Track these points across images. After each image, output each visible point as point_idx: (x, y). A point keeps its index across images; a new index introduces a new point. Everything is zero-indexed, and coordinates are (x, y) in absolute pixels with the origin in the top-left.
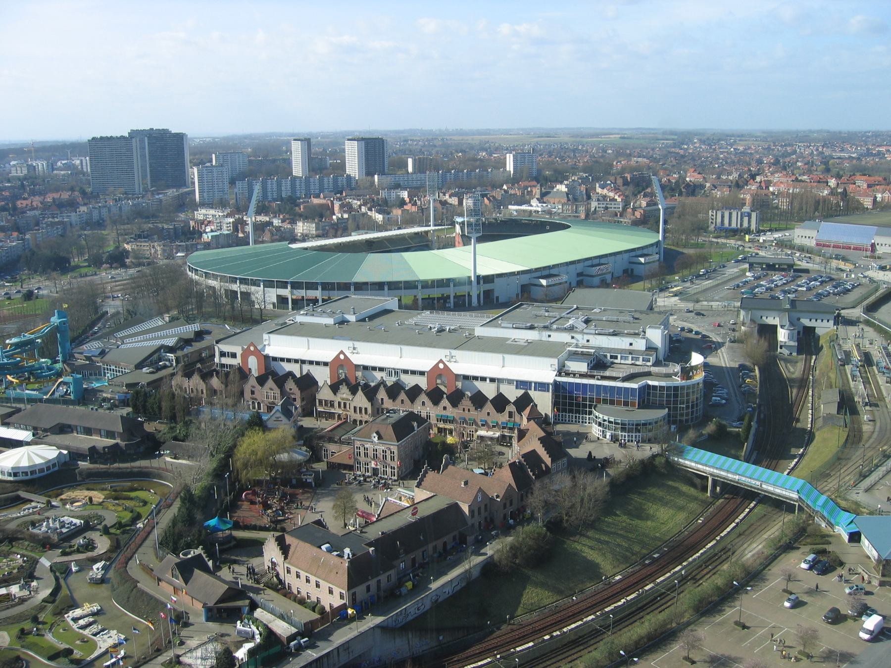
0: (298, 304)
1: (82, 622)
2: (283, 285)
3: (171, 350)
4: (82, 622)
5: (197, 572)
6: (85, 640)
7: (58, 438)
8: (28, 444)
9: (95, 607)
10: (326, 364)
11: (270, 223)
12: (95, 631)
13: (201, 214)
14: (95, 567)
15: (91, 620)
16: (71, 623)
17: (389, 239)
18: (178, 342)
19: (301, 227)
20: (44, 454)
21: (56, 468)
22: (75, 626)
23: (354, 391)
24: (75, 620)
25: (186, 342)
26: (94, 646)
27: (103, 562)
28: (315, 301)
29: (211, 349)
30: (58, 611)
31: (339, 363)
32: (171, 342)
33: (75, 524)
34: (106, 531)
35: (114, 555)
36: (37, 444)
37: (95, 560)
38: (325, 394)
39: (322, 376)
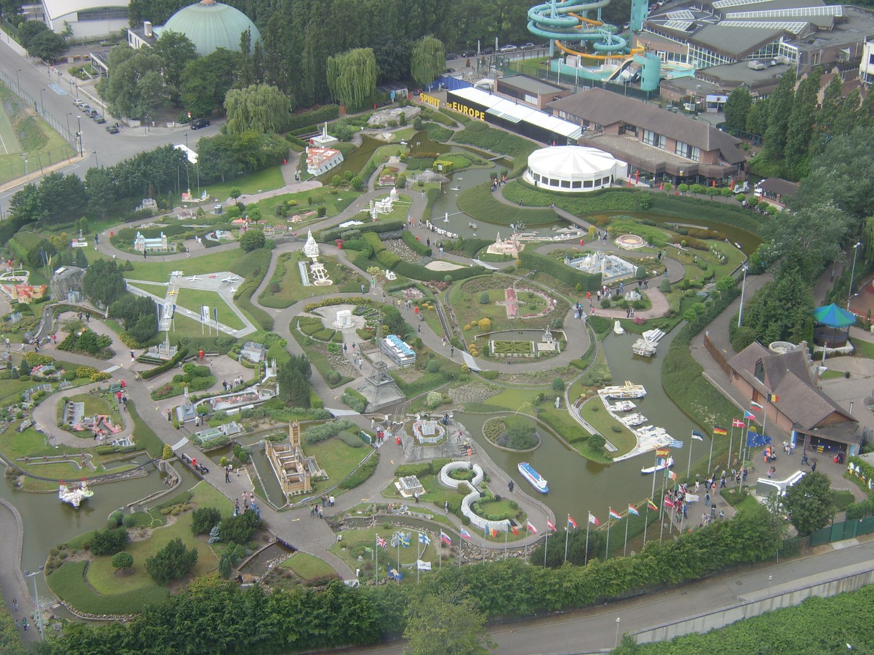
1: (620, 406)
3: (790, 37)
4: (620, 406)
5: (790, 376)
6: (618, 430)
7: (617, 142)
8: (574, 143)
9: (640, 391)
12: (637, 421)
14: (645, 334)
15: (632, 405)
16: (606, 403)
18: (804, 31)
22: (610, 409)
24: (612, 400)
26: (632, 442)
27: (657, 331)
30: (590, 381)
32: (796, 27)
33: (625, 269)
34: (666, 289)
35: (673, 322)
36: (586, 145)
37: (646, 325)
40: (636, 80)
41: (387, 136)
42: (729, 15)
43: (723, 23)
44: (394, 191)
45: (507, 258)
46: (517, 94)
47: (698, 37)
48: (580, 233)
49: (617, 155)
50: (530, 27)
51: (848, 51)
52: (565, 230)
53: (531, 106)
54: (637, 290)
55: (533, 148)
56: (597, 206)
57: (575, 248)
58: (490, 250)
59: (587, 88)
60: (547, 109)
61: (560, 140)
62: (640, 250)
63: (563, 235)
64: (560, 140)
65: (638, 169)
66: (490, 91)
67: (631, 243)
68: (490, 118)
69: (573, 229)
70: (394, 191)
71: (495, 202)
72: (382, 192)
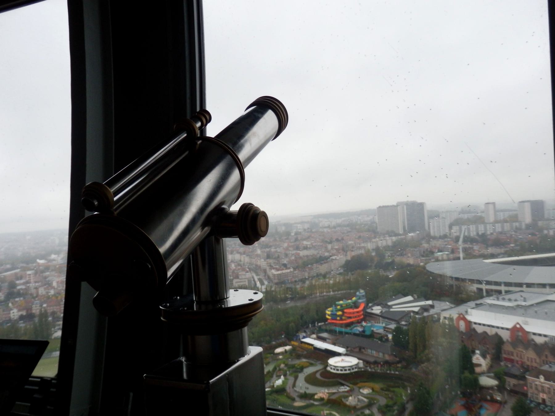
0: (489, 293)
2: (480, 282)
3: (417, 313)
10: (507, 329)
11: (472, 248)
13: (433, 243)
17: (548, 258)
18: (419, 310)
19: (490, 250)
20: (352, 361)
21: (356, 370)
23: (526, 348)
25: (425, 309)
28: (500, 292)
29: (439, 314)
31: (516, 330)
32: (416, 309)
38: (507, 348)
39: (505, 336)
40: (364, 331)
41: (281, 357)
42: (394, 307)
43: (392, 310)
44: (282, 377)
45: (322, 399)
46: (323, 340)
47: (384, 315)
48: (348, 388)
49: (359, 359)
50: (327, 317)
51: (436, 316)
52: (343, 387)
53: (329, 343)
54: (369, 409)
55: (328, 358)
56: (353, 378)
57: (346, 394)
58: (316, 397)
59: (347, 335)
60: (334, 344)
61: (339, 354)
62: (369, 394)
63: (343, 389)
64: (339, 354)
65: (366, 362)
66: (315, 339)
67: (366, 391)
68: (316, 349)
69: (346, 387)
70: (282, 377)
71: (317, 378)
72: (279, 377)
